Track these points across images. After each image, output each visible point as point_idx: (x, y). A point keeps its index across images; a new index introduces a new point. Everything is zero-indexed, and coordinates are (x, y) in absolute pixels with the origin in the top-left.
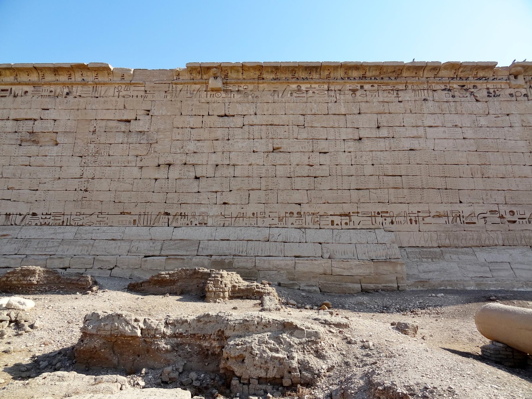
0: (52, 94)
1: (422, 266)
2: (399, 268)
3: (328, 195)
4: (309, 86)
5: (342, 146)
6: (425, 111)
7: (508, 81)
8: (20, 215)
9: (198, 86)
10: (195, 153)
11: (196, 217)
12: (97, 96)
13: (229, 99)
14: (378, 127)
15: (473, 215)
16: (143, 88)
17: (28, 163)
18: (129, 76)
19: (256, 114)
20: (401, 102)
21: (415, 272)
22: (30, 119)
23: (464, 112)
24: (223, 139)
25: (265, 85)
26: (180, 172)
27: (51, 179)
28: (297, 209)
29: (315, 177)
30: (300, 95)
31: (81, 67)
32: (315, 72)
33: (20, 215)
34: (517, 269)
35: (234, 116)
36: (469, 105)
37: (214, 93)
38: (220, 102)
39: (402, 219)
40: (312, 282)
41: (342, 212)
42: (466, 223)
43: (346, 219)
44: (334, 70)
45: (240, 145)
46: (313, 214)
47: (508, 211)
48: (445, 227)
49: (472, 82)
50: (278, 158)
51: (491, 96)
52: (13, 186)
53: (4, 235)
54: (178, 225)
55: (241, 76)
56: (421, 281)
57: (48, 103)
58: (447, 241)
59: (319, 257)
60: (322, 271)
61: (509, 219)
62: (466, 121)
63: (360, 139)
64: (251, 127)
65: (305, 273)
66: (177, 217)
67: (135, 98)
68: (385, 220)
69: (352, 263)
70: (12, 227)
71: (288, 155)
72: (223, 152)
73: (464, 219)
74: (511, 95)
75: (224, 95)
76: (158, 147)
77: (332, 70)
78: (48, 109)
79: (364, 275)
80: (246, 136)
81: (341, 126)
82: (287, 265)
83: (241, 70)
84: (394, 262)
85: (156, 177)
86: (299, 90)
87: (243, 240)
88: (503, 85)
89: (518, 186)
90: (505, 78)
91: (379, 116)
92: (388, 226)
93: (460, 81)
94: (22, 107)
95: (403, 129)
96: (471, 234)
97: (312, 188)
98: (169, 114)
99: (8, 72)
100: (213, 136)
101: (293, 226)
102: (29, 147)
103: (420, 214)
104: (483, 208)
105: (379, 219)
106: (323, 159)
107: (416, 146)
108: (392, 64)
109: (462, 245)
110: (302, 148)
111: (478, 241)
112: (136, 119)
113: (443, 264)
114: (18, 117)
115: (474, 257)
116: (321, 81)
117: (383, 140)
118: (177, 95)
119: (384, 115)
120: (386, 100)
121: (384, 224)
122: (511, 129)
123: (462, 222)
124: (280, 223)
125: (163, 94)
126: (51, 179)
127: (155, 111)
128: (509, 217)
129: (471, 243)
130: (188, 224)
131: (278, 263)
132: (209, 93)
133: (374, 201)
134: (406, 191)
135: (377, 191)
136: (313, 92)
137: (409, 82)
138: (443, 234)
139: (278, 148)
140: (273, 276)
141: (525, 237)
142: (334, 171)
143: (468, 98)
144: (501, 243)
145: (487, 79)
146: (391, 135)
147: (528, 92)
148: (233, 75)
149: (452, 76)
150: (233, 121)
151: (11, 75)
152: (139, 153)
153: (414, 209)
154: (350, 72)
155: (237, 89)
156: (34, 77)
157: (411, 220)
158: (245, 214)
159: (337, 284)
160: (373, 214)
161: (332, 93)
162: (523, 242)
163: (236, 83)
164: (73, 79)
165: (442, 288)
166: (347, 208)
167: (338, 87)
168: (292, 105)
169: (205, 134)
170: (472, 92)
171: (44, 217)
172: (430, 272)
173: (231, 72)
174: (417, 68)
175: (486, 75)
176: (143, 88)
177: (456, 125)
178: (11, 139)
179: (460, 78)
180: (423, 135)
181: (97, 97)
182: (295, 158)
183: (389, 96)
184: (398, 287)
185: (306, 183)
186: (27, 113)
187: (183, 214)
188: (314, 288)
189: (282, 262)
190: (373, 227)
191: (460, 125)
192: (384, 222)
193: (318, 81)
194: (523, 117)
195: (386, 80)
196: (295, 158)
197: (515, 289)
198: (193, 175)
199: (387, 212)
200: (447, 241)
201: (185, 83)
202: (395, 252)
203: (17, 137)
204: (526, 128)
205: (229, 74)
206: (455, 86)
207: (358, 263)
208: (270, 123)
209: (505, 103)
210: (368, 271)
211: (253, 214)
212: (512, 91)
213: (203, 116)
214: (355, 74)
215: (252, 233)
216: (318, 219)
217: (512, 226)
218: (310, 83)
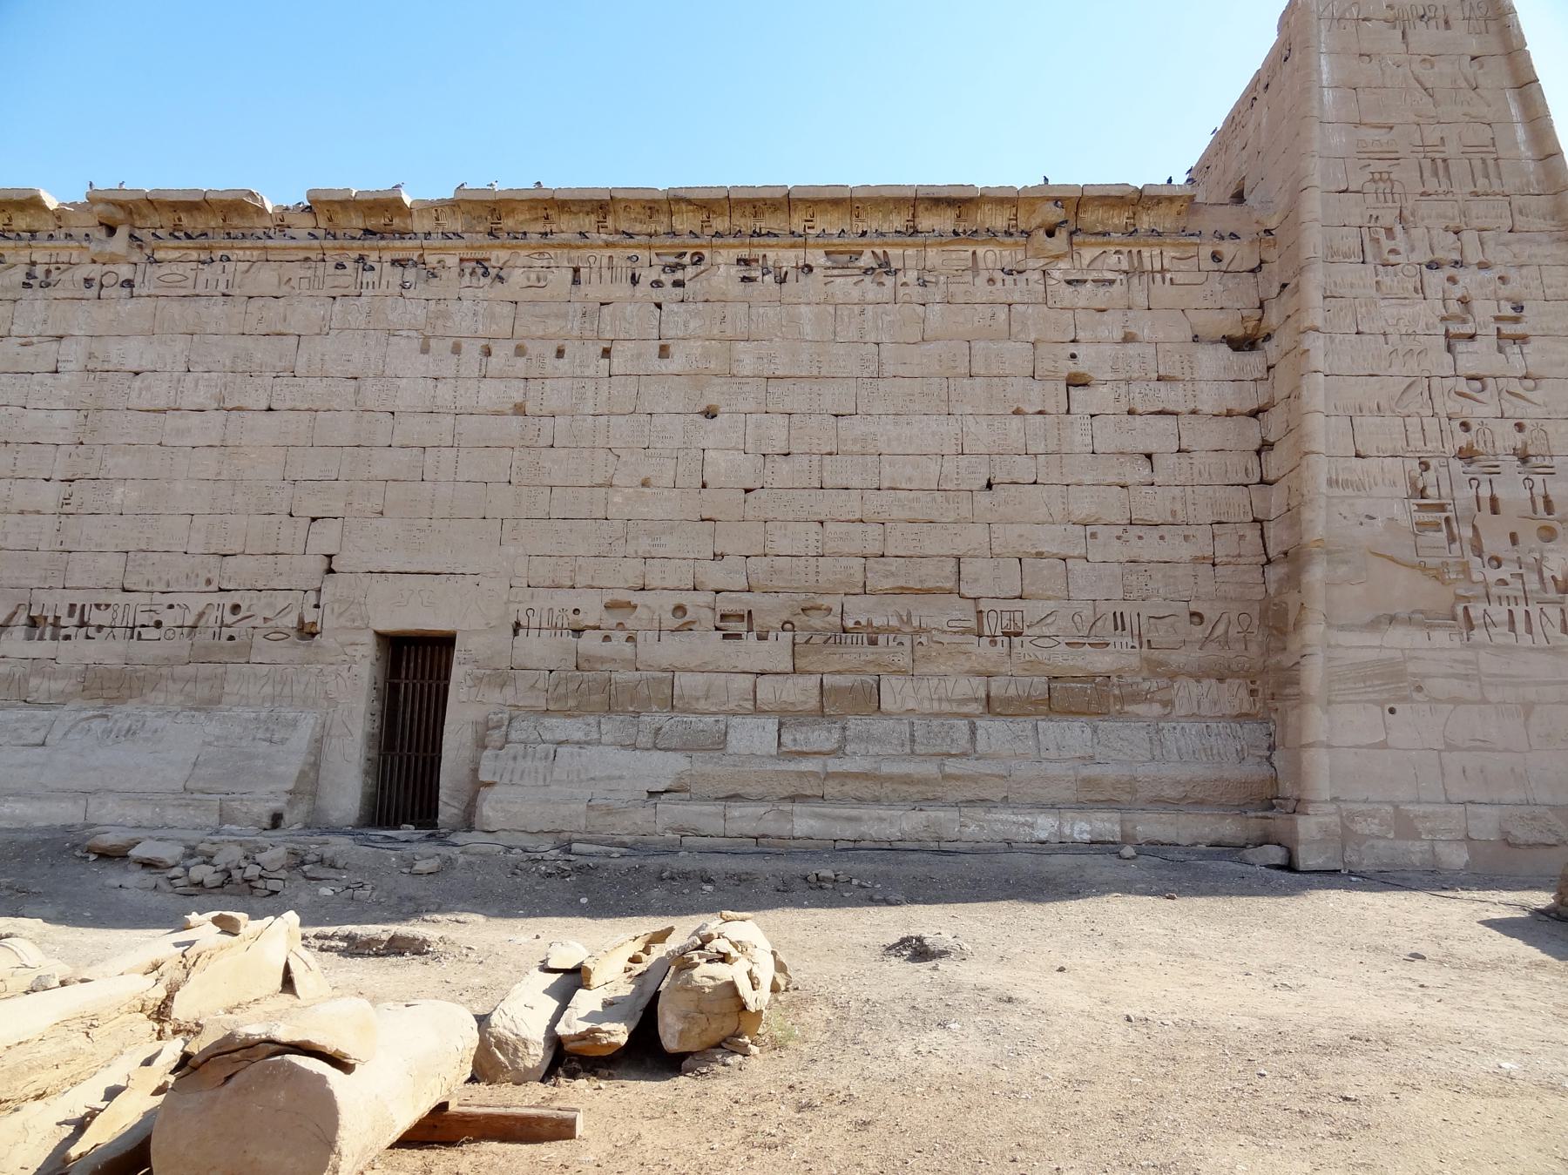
88: (75, 253)
122: (49, 379)
147: (139, 273)
175: (36, 226)
212: (95, 271)
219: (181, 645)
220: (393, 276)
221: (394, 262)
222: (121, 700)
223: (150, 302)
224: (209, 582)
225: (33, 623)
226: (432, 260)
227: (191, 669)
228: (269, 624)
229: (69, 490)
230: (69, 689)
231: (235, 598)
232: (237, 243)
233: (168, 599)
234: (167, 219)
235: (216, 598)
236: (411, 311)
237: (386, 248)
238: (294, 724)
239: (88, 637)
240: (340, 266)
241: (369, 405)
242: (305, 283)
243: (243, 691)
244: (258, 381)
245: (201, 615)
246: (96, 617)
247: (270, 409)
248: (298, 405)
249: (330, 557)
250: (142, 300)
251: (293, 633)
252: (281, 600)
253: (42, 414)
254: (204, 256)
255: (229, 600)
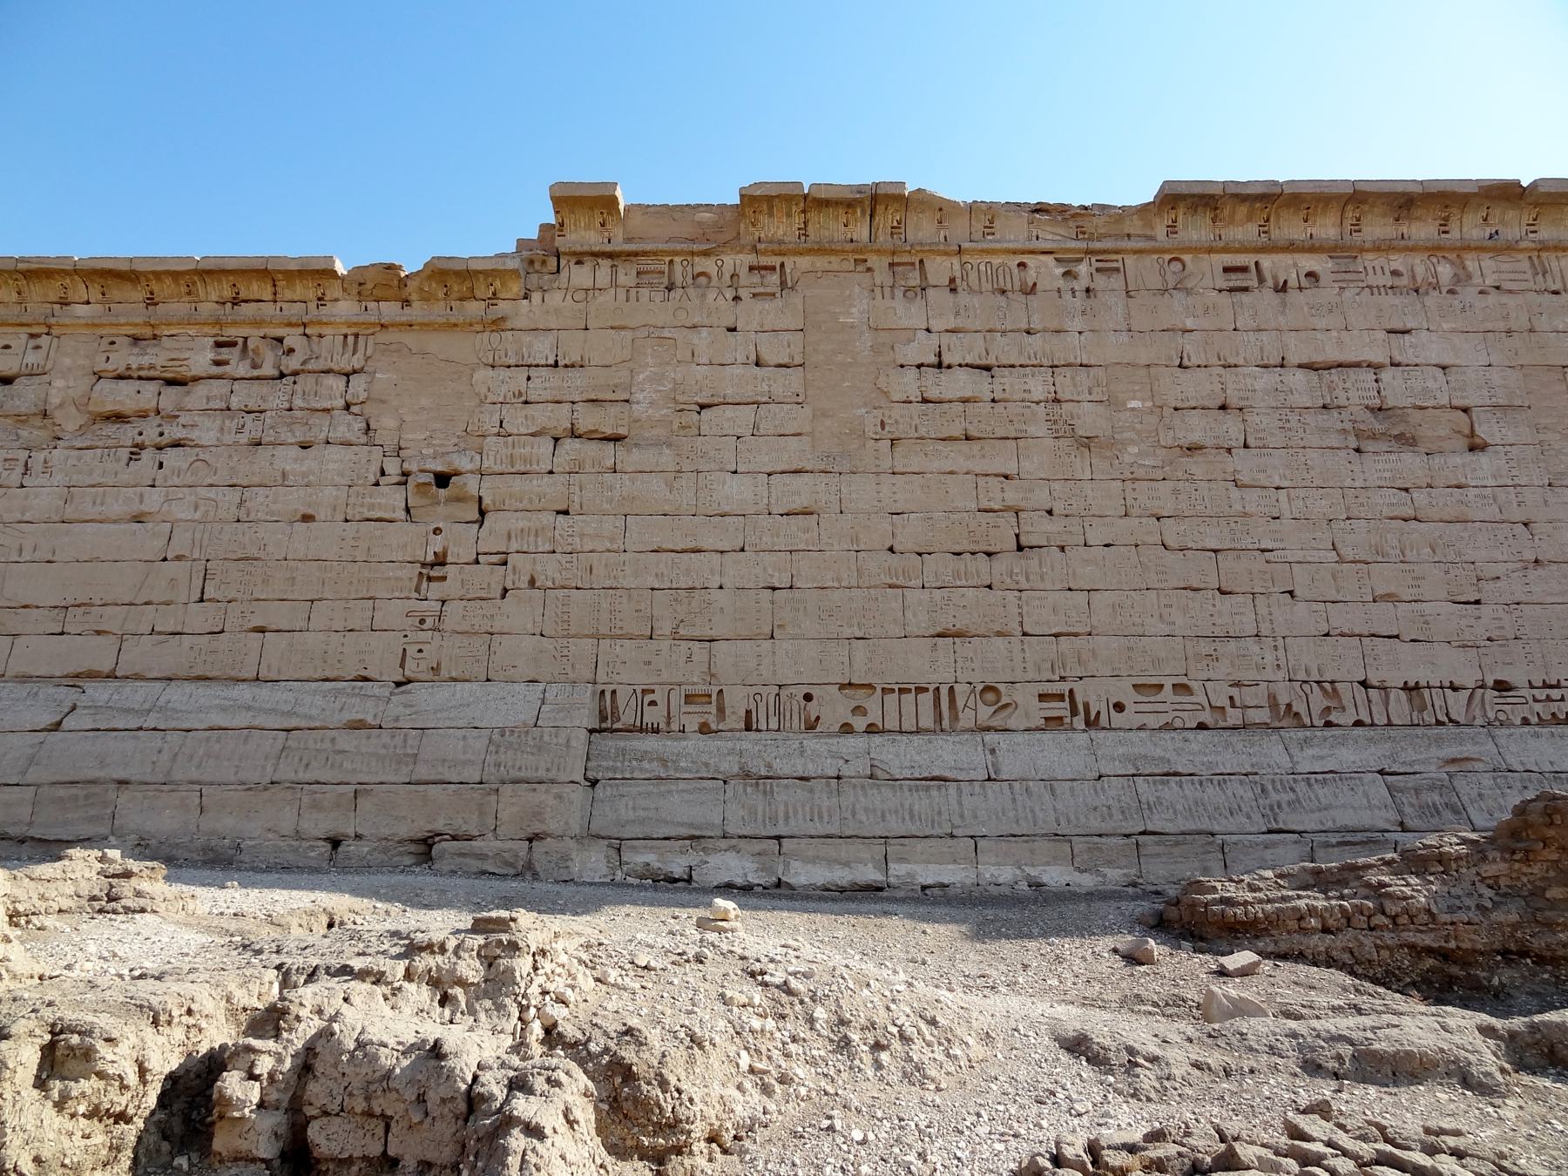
0: (1404, 281)
8: (1454, 688)
12: (1554, 288)
17: (1411, 513)
22: (1357, 365)
27: (1511, 566)
31: (1506, 194)
33: (1454, 688)
52: (1392, 589)
53: (1454, 761)
57: (1401, 309)
70: (1442, 730)
78: (1408, 332)
94: (1321, 323)
99: (1243, 210)
102: (1393, 457)
114: (1318, 358)
126: (1511, 566)
151: (1250, 219)
156: (1326, 228)
164: (1455, 234)
171: (1541, 694)
178: (1325, 431)
181: (1556, 293)
186: (1340, 342)
203: (1339, 426)
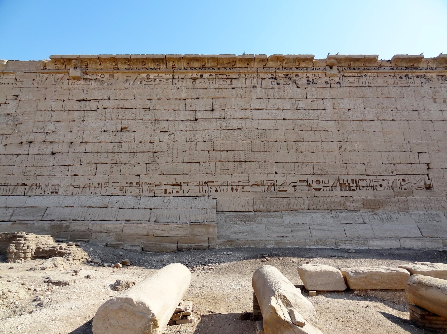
1: (235, 228)
2: (211, 230)
3: (164, 167)
4: (156, 75)
5: (179, 126)
6: (254, 96)
7: (324, 71)
9: (62, 75)
10: (54, 132)
11: (49, 187)
13: (88, 86)
14: (213, 110)
15: (285, 184)
16: (14, 77)
18: (3, 66)
19: (109, 99)
20: (234, 88)
21: (228, 233)
23: (285, 97)
24: (79, 120)
25: (119, 74)
26: (39, 148)
28: (137, 179)
29: (155, 152)
30: (148, 83)
32: (162, 63)
34: (314, 229)
35: (90, 100)
36: (291, 91)
37: (75, 81)
38: (80, 89)
39: (225, 188)
40: (136, 243)
41: (174, 182)
42: (279, 191)
43: (177, 188)
44: (178, 61)
45: (93, 125)
46: (151, 184)
47: (314, 181)
48: (261, 195)
49: (295, 71)
50: (125, 136)
51: (309, 84)
54: (33, 194)
55: (99, 67)
56: (230, 241)
58: (262, 206)
59: (146, 221)
60: (145, 233)
61: (315, 188)
62: (287, 105)
63: (196, 120)
64: (104, 110)
65: (131, 235)
66: (32, 187)
67: (6, 85)
68: (211, 188)
69: (171, 226)
71: (132, 134)
72: (78, 132)
73: (277, 188)
74: (326, 83)
75: (83, 82)
76: (22, 127)
77: (176, 61)
79: (181, 236)
80: (99, 118)
81: (180, 109)
82: (116, 228)
83: (98, 61)
84: (207, 225)
85: (18, 153)
86: (148, 79)
87: (85, 207)
88: (320, 74)
89: (325, 159)
90: (322, 68)
91: (214, 100)
92: (213, 194)
93: (284, 71)
95: (233, 111)
96: (282, 200)
97: (151, 162)
98: (34, 99)
100: (70, 118)
101: (131, 194)
103: (240, 183)
104: (295, 178)
105: (206, 188)
106: (164, 137)
107: (242, 125)
108: (225, 57)
109: (273, 210)
110: (146, 127)
111: (287, 206)
112: (6, 104)
113: (253, 226)
115: (281, 220)
116: (167, 70)
117: (215, 120)
118: (43, 83)
119: (218, 99)
120: (221, 86)
121: (209, 192)
122: (323, 111)
123: (276, 190)
124: (120, 192)
125: (31, 82)
127: (22, 96)
128: (315, 186)
129: (282, 208)
130: (41, 194)
131: (108, 226)
132: (71, 81)
133: (202, 173)
134: (230, 164)
135: (206, 164)
136: (160, 80)
137: (241, 71)
138: (258, 201)
139: (126, 128)
140: (103, 238)
141: (327, 202)
142: (171, 147)
143: (291, 85)
144: (306, 207)
145: (307, 69)
146: (222, 117)
147: (341, 80)
148: (92, 66)
149: (278, 67)
150: (89, 105)
152: (5, 133)
153: (236, 179)
154: (192, 63)
155: (95, 78)
157: (232, 188)
158: (91, 185)
159: (157, 244)
160: (201, 183)
161: (176, 81)
162: (325, 207)
163: (93, 73)
165: (247, 246)
166: (179, 179)
167: (182, 76)
168: (141, 91)
169: (64, 116)
170: (294, 80)
172: (240, 233)
173: (91, 63)
174: (248, 60)
175: (307, 66)
176: (14, 77)
177: (278, 108)
179: (285, 68)
180: (250, 116)
182: (139, 136)
183: (224, 83)
184: (209, 245)
185: (146, 157)
187: (38, 185)
188: (136, 248)
189: (112, 226)
190: (200, 194)
191: (282, 108)
192: (210, 190)
193: (164, 71)
194: (334, 101)
195: (222, 70)
196: (139, 136)
197: (308, 247)
198: (50, 151)
199: (213, 182)
200: (262, 206)
201: (50, 73)
202: (213, 215)
204: (336, 110)
205: (89, 65)
206: (280, 75)
207: (176, 225)
208: (121, 106)
209: (321, 89)
210: (184, 233)
211: (99, 184)
212: (328, 79)
213: (64, 100)
214: (196, 65)
215: (95, 201)
216: (154, 188)
217: (317, 193)
218: (157, 72)
219: (389, 192)
220: (418, 81)
221: (417, 77)
222: (377, 209)
223: (347, 89)
224: (392, 172)
225: (341, 185)
226: (428, 76)
227: (396, 199)
228: (416, 185)
229: (340, 145)
230: (360, 206)
231: (403, 177)
232: (370, 71)
233: (382, 178)
234: (346, 64)
235: (397, 177)
236: (426, 90)
237: (414, 72)
238: (438, 215)
239: (360, 190)
240: (400, 77)
241: (424, 118)
242: (392, 83)
243: (415, 206)
244: (388, 111)
245: (393, 182)
246: (361, 183)
247: (393, 120)
248: (402, 119)
249: (427, 164)
250: (344, 88)
251: (424, 188)
252: (418, 178)
253: (325, 122)
254: (359, 75)
255: (401, 178)
